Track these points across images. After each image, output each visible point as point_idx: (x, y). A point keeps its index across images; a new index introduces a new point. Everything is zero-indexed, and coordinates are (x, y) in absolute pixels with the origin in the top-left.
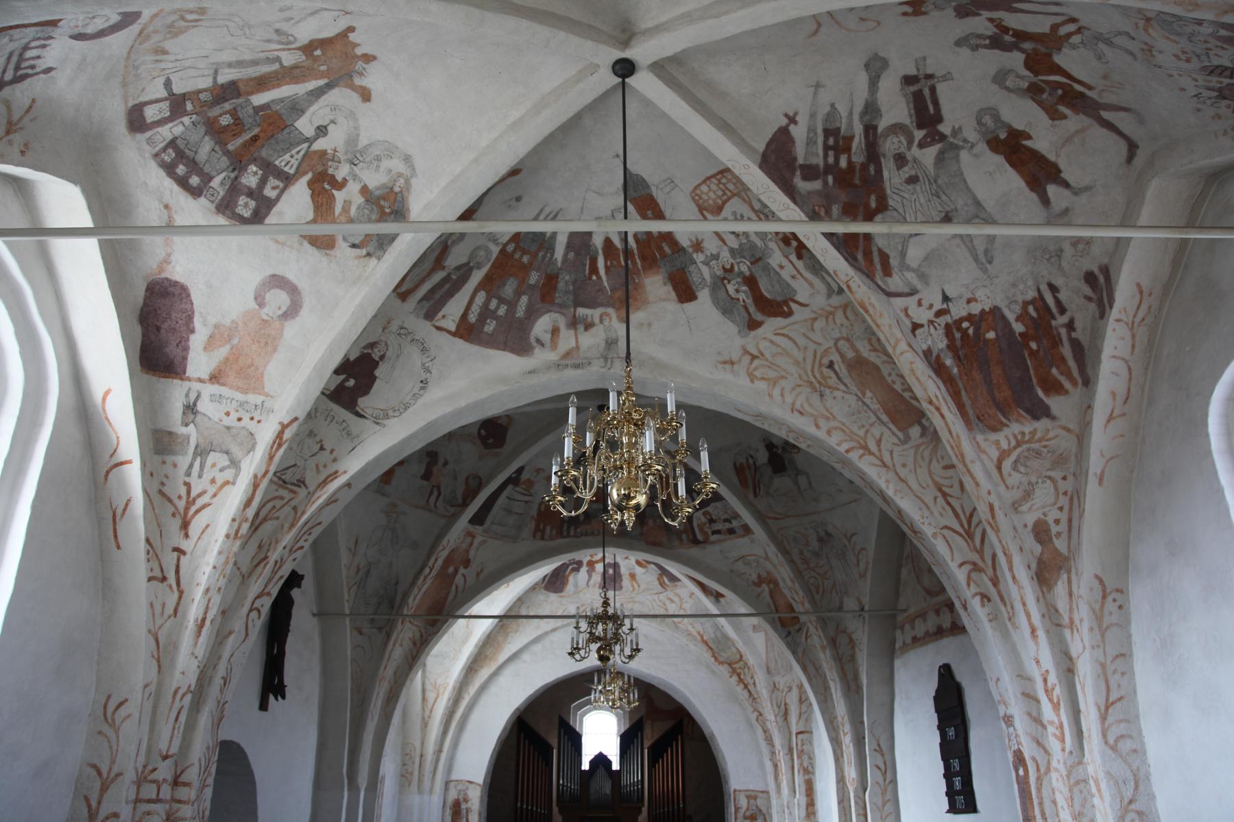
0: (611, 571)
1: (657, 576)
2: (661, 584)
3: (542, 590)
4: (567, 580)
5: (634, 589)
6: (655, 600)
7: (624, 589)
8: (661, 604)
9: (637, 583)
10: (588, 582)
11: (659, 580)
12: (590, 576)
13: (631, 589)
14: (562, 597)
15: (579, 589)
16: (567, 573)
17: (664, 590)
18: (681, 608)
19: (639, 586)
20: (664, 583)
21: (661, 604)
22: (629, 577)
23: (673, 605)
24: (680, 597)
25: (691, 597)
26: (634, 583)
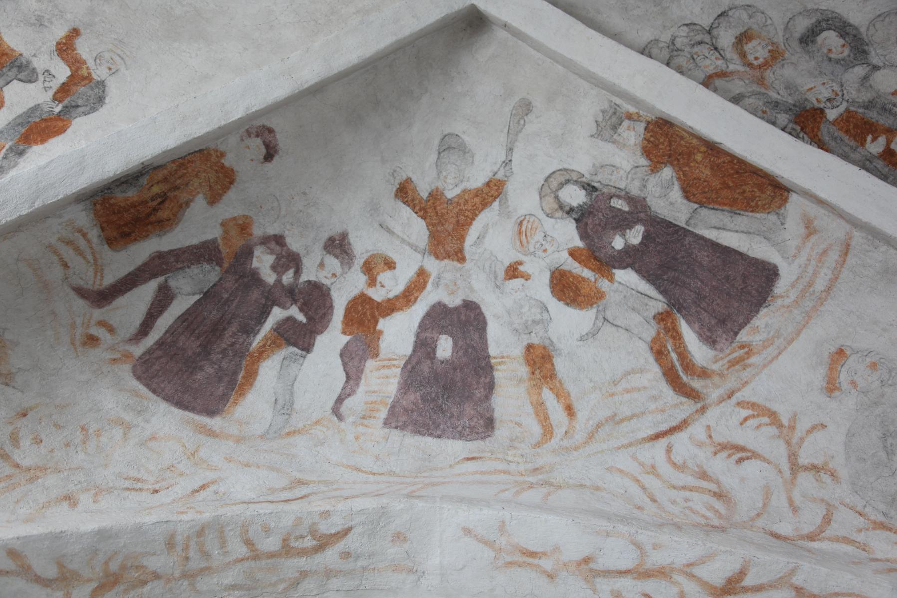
0: (445, 347)
1: (650, 331)
2: (671, 377)
3: (126, 370)
4: (252, 375)
5: (548, 431)
6: (653, 470)
7: (502, 432)
8: (688, 480)
9: (560, 394)
10: (340, 400)
11: (659, 354)
12: (353, 377)
13: (536, 429)
14: (211, 433)
15: (297, 422)
16: (257, 341)
17: (688, 407)
18: (795, 468)
19: (570, 410)
20: (688, 366)
21: (688, 480)
22: (523, 370)
23: (752, 468)
24: (773, 415)
25: (831, 387)
26: (547, 395)
